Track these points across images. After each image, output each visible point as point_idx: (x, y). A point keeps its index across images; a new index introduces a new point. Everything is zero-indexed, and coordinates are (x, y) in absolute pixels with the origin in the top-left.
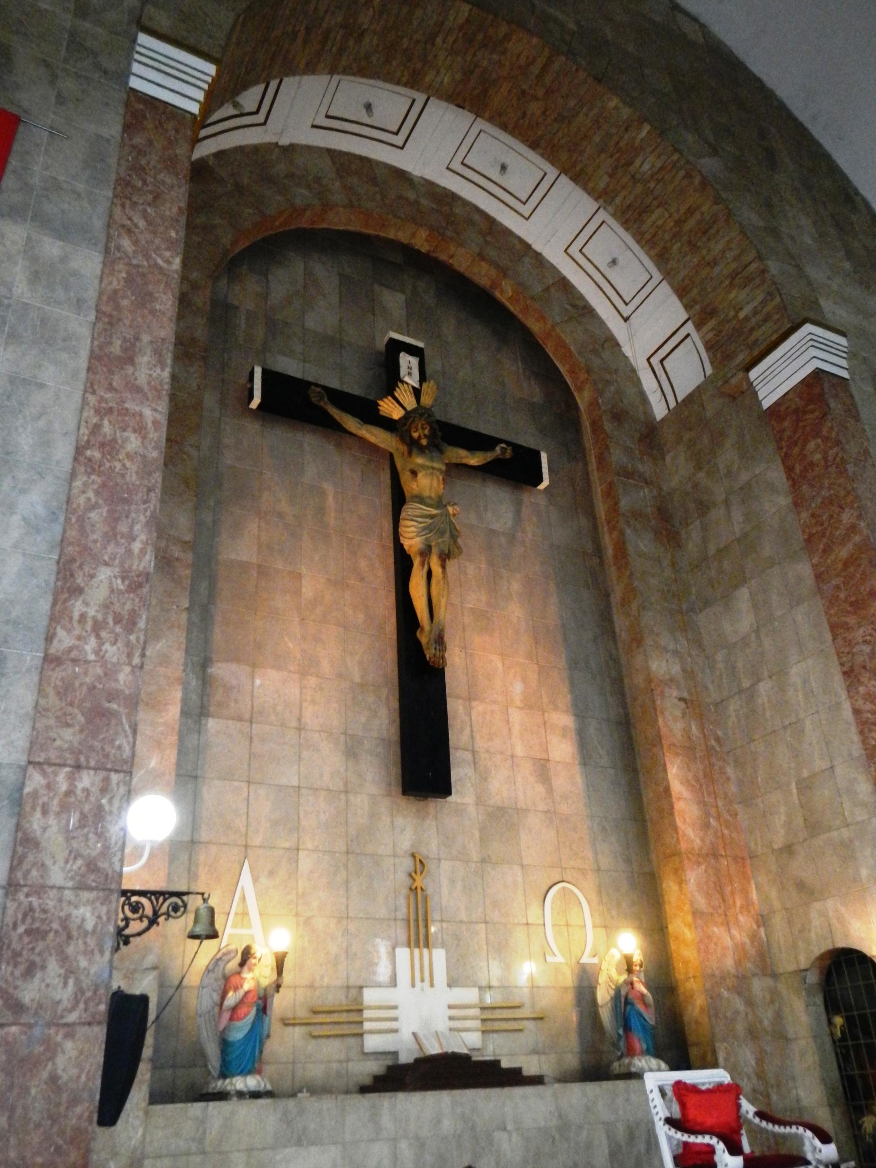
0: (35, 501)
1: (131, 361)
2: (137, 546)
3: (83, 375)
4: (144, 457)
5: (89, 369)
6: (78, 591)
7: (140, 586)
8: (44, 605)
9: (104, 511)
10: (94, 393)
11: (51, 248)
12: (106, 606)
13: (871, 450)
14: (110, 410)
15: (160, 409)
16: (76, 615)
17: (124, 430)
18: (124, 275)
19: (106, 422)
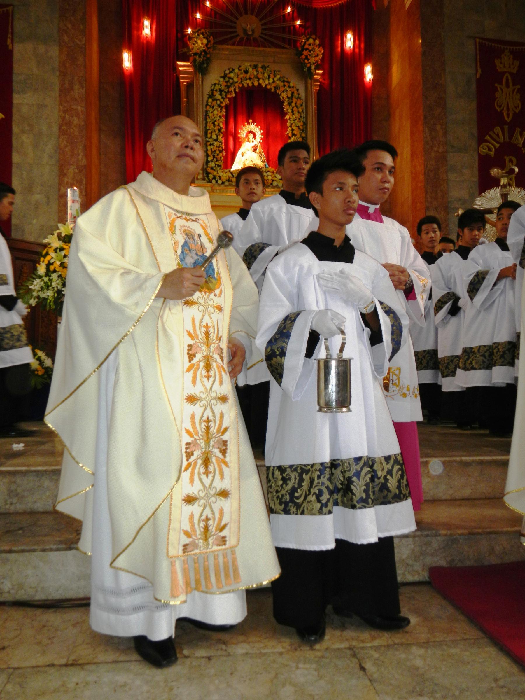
0: (50, 147)
1: (72, 89)
2: (80, 157)
3: (58, 99)
4: (79, 125)
5: (60, 95)
6: (65, 175)
7: (82, 170)
8: (57, 181)
9: (69, 147)
10: (62, 105)
11: (42, 49)
12: (73, 178)
13: (443, 34)
14: (67, 110)
15: (83, 105)
16: (66, 182)
17: (72, 117)
18: (66, 53)
19: (67, 115)
